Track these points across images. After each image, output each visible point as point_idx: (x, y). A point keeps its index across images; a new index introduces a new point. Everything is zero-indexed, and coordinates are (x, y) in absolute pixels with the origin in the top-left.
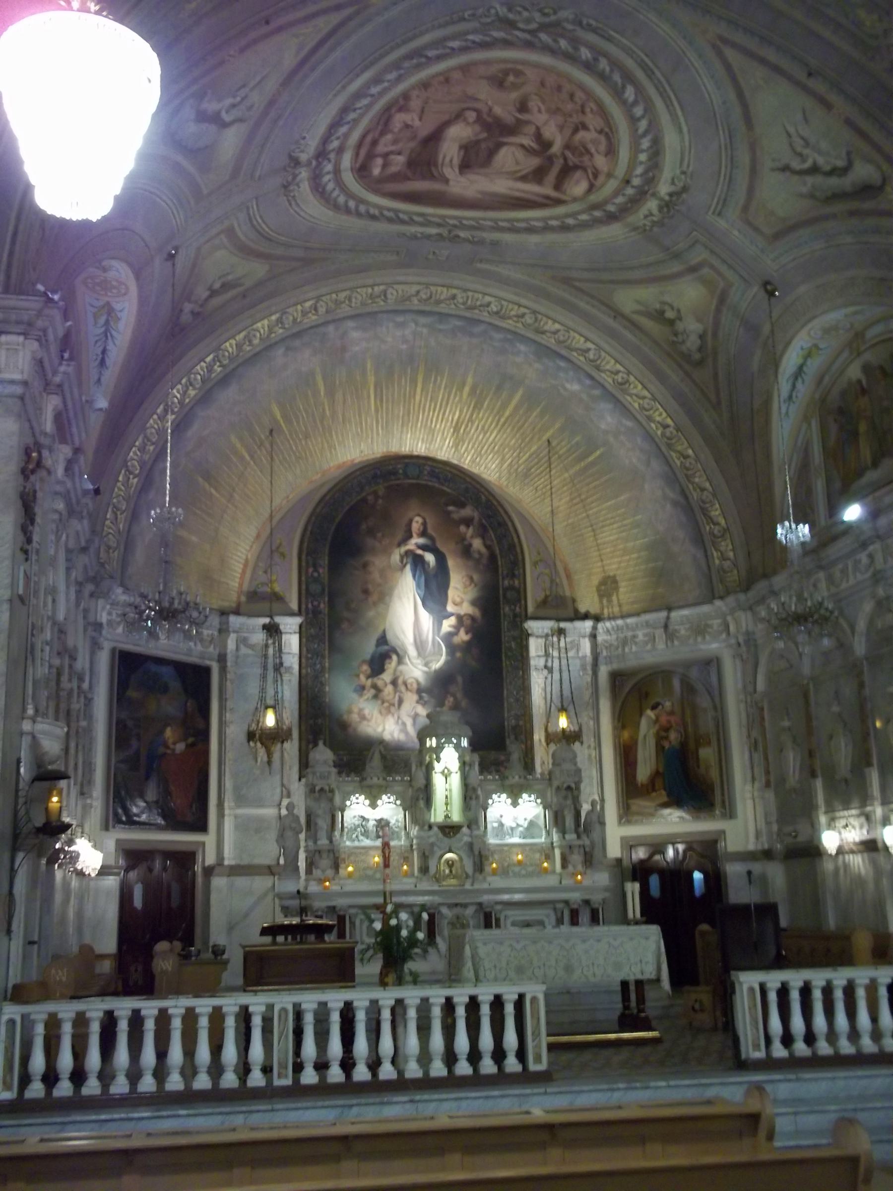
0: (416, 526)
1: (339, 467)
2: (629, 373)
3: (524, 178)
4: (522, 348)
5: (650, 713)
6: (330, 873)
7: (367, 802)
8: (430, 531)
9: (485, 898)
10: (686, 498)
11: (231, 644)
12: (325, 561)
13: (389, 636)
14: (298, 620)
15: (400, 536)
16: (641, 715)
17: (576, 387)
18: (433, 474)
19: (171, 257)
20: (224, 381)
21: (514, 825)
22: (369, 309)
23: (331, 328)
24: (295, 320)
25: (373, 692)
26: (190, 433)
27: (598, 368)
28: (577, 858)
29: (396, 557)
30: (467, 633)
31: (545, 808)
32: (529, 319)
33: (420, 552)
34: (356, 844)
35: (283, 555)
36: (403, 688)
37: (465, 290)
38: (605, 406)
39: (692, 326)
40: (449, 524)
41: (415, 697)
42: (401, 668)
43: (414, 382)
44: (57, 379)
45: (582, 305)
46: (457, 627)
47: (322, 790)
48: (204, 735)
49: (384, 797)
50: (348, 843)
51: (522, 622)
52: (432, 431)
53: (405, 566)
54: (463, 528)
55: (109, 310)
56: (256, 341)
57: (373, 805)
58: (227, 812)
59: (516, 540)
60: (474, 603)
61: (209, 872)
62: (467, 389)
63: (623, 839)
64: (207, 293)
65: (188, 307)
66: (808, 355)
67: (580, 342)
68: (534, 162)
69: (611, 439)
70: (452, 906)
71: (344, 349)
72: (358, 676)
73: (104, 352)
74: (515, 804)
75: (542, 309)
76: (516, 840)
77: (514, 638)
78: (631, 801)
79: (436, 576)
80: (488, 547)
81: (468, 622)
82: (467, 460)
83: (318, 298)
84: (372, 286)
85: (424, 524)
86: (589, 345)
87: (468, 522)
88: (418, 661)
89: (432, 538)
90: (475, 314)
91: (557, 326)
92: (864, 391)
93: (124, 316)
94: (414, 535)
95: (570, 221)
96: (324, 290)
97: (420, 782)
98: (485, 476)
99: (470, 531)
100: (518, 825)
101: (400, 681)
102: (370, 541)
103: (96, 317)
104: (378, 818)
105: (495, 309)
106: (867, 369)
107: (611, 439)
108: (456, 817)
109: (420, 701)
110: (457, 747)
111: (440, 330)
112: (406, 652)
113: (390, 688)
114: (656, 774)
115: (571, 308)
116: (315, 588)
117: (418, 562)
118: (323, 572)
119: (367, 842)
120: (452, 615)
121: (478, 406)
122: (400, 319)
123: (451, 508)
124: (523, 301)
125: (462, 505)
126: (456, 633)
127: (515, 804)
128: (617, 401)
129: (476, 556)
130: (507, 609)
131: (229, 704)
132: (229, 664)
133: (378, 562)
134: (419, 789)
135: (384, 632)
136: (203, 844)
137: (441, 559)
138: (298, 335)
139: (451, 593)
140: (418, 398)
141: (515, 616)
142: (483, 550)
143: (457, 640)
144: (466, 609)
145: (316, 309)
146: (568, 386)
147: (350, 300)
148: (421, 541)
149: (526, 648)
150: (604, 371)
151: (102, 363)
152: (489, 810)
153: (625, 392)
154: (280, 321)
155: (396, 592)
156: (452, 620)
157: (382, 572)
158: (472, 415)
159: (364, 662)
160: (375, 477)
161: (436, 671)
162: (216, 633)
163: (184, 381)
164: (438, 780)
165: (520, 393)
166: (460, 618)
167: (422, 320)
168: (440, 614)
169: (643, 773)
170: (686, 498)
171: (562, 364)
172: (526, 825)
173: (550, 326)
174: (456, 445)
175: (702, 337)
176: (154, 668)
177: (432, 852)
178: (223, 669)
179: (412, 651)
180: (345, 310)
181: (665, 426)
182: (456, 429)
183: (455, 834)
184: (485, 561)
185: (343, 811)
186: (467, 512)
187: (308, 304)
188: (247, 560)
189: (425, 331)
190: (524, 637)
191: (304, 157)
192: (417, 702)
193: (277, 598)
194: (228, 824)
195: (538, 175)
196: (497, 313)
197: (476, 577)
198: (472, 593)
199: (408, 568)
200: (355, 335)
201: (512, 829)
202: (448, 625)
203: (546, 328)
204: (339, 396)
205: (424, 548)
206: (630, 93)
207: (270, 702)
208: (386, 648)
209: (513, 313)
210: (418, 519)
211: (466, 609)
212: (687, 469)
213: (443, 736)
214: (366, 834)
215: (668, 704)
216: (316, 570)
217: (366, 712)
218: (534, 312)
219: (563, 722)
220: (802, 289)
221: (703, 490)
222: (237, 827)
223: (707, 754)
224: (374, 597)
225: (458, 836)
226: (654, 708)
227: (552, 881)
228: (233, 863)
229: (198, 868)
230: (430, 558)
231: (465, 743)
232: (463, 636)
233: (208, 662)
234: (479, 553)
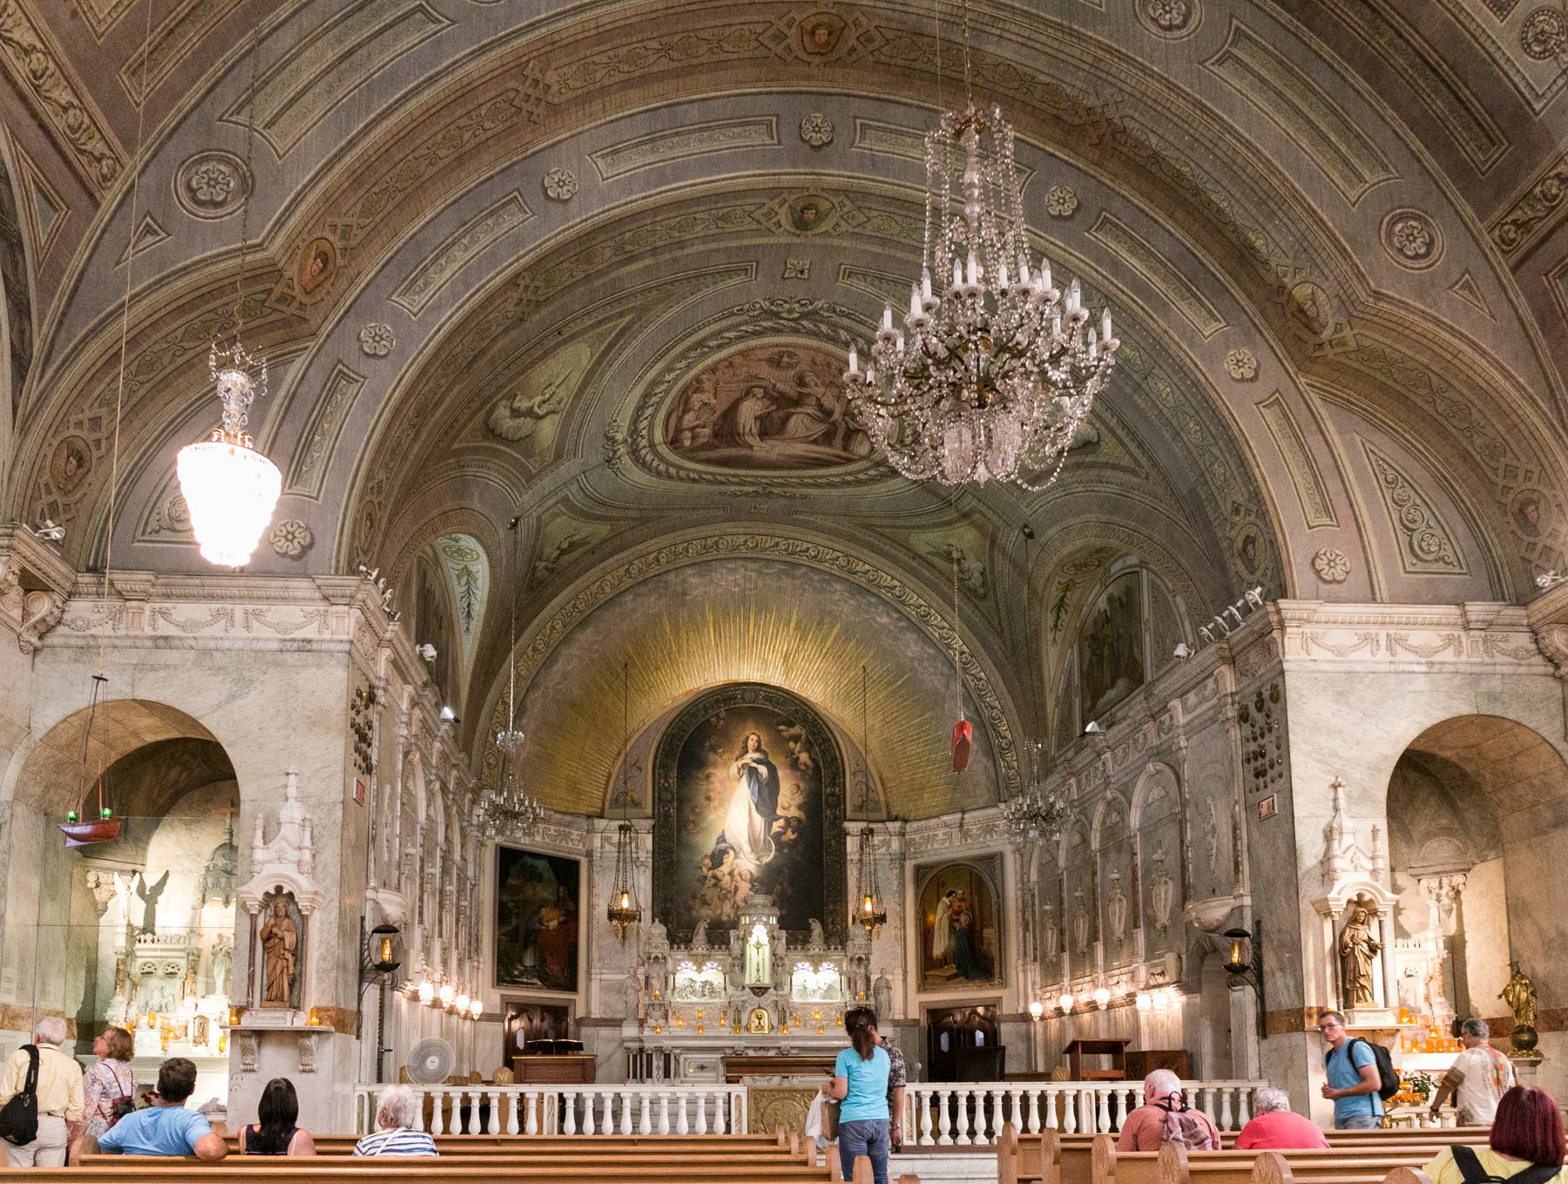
0: (752, 743)
1: (687, 694)
2: (930, 606)
4: (838, 587)
8: (763, 747)
10: (979, 716)
12: (674, 773)
13: (727, 836)
14: (651, 822)
15: (737, 753)
17: (885, 620)
18: (767, 699)
19: (514, 525)
20: (582, 625)
22: (704, 558)
23: (672, 575)
24: (640, 570)
26: (555, 669)
27: (903, 602)
29: (734, 768)
32: (842, 562)
33: (754, 765)
35: (640, 769)
36: (738, 878)
37: (786, 539)
38: (910, 636)
39: (973, 565)
40: (780, 741)
41: (749, 886)
42: (737, 861)
43: (747, 619)
45: (886, 548)
46: (785, 828)
48: (572, 917)
51: (841, 823)
52: (765, 662)
54: (792, 744)
55: (467, 571)
56: (607, 589)
60: (799, 807)
61: (579, 1023)
62: (792, 625)
64: (558, 552)
65: (541, 565)
66: (1067, 588)
67: (887, 581)
69: (916, 663)
71: (684, 593)
75: (853, 553)
77: (834, 837)
79: (767, 785)
80: (813, 760)
81: (795, 823)
82: (795, 685)
83: (660, 550)
85: (759, 741)
86: (895, 583)
87: (796, 739)
88: (752, 857)
89: (765, 753)
90: (795, 559)
91: (867, 567)
92: (1108, 620)
93: (479, 575)
96: (664, 544)
101: (736, 873)
102: (712, 757)
103: (459, 578)
106: (1110, 599)
107: (916, 663)
111: (767, 574)
113: (728, 877)
115: (878, 551)
116: (665, 795)
117: (753, 772)
118: (673, 781)
120: (781, 817)
121: (803, 639)
122: (732, 565)
123: (781, 727)
124: (837, 546)
125: (791, 724)
126: (785, 833)
128: (919, 631)
129: (803, 767)
133: (718, 774)
138: (644, 582)
139: (780, 799)
141: (835, 818)
142: (809, 762)
143: (784, 838)
144: (794, 812)
146: (878, 619)
148: (756, 755)
150: (909, 605)
151: (469, 615)
153: (927, 623)
154: (627, 571)
156: (781, 822)
157: (722, 782)
160: (717, 701)
163: (548, 626)
165: (839, 626)
166: (787, 820)
167: (751, 565)
168: (770, 817)
170: (979, 716)
171: (873, 600)
173: (861, 567)
175: (982, 574)
176: (530, 861)
179: (747, 848)
180: (683, 561)
181: (962, 653)
182: (786, 658)
184: (810, 772)
186: (796, 730)
189: (753, 575)
194: (595, 987)
196: (815, 557)
197: (802, 785)
198: (799, 799)
199: (744, 777)
200: (695, 581)
202: (777, 826)
203: (858, 569)
204: (683, 635)
205: (758, 762)
208: (723, 846)
210: (755, 738)
211: (794, 812)
212: (980, 690)
216: (667, 781)
217: (708, 898)
218: (847, 556)
219: (868, 907)
220: (1051, 532)
221: (993, 708)
222: (601, 989)
224: (715, 803)
228: (598, 1016)
229: (570, 1020)
230: (763, 770)
232: (790, 835)
234: (805, 765)
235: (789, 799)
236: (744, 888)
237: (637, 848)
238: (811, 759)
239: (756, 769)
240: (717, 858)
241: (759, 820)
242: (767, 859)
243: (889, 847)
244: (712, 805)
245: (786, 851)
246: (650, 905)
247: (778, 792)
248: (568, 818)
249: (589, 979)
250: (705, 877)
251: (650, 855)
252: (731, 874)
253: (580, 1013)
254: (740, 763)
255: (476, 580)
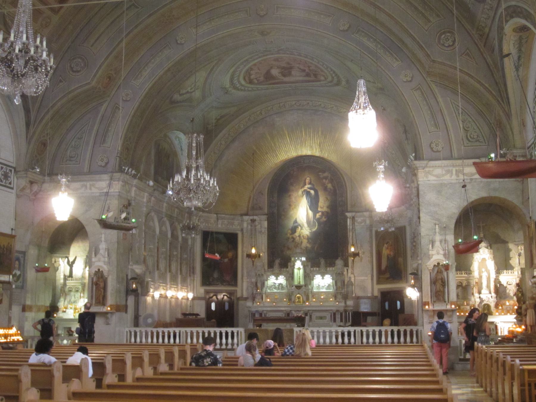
0: (307, 181)
1: (281, 162)
3: (305, 76)
5: (386, 245)
6: (260, 300)
7: (275, 278)
8: (312, 182)
9: (304, 309)
11: (245, 225)
12: (276, 195)
13: (298, 220)
15: (302, 185)
16: (383, 246)
19: (192, 121)
20: (233, 141)
21: (324, 285)
25: (292, 239)
28: (339, 296)
29: (300, 192)
30: (325, 218)
31: (333, 280)
33: (309, 190)
34: (272, 291)
35: (262, 194)
37: (312, 101)
42: (302, 231)
43: (301, 132)
44: (134, 183)
46: (322, 216)
47: (259, 274)
49: (280, 276)
50: (269, 291)
52: (311, 147)
53: (303, 195)
54: (324, 180)
56: (242, 127)
57: (277, 279)
58: (244, 280)
59: (344, 184)
60: (328, 207)
61: (238, 299)
62: (320, 133)
63: (379, 289)
68: (304, 74)
70: (295, 311)
72: (287, 234)
73: (181, 146)
74: (323, 278)
76: (324, 290)
78: (380, 276)
80: (334, 187)
82: (326, 155)
84: (279, 103)
85: (310, 180)
87: (326, 178)
88: (308, 229)
89: (313, 185)
94: (307, 184)
95: (327, 85)
97: (291, 272)
98: (332, 161)
99: (327, 181)
100: (325, 286)
101: (301, 236)
104: (279, 283)
105: (323, 106)
108: (302, 283)
109: (308, 242)
110: (301, 261)
112: (303, 225)
113: (298, 238)
114: (387, 267)
117: (308, 194)
119: (275, 291)
120: (320, 212)
123: (320, 174)
125: (324, 172)
127: (323, 278)
130: (340, 209)
131: (245, 245)
132: (244, 232)
133: (294, 195)
134: (290, 274)
135: (296, 219)
136: (236, 290)
137: (316, 192)
138: (257, 122)
140: (304, 137)
142: (332, 188)
145: (261, 113)
147: (272, 108)
148: (309, 186)
149: (347, 222)
151: (182, 149)
152: (314, 280)
154: (249, 119)
155: (300, 205)
156: (320, 213)
158: (324, 141)
159: (289, 229)
161: (314, 232)
162: (240, 222)
163: (219, 143)
164: (296, 271)
166: (323, 213)
169: (383, 267)
172: (327, 285)
174: (321, 151)
177: (292, 294)
178: (243, 233)
179: (306, 225)
182: (320, 145)
183: (300, 289)
185: (267, 281)
187: (258, 113)
188: (250, 198)
190: (346, 218)
191: (227, 86)
192: (307, 242)
193: (261, 208)
195: (308, 75)
196: (324, 107)
198: (327, 204)
199: (305, 196)
201: (323, 287)
202: (318, 216)
206: (315, 60)
207: (253, 245)
208: (296, 224)
209: (329, 107)
211: (325, 209)
213: (297, 257)
214: (275, 288)
215: (391, 242)
223: (401, 260)
224: (293, 206)
225: (302, 289)
226: (387, 244)
227: (332, 304)
230: (312, 192)
231: (304, 259)
232: (324, 219)
233: (238, 232)
234: (330, 189)
235: (323, 204)
236: (305, 242)
237: (261, 227)
238: (332, 186)
239: (309, 192)
240: (294, 230)
241: (311, 213)
242: (314, 230)
243: (365, 222)
244: (291, 208)
245: (322, 225)
246: (266, 250)
247: (318, 202)
248: (232, 216)
249: (243, 282)
250: (289, 238)
251: (266, 230)
252: (299, 236)
253: (239, 295)
254: (303, 190)
255: (181, 139)
